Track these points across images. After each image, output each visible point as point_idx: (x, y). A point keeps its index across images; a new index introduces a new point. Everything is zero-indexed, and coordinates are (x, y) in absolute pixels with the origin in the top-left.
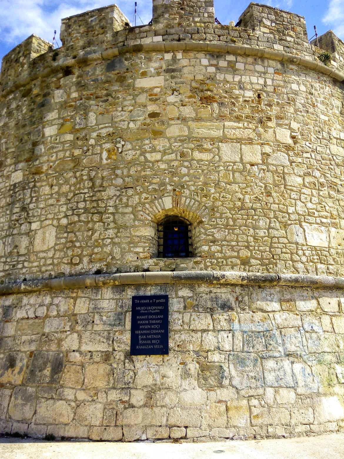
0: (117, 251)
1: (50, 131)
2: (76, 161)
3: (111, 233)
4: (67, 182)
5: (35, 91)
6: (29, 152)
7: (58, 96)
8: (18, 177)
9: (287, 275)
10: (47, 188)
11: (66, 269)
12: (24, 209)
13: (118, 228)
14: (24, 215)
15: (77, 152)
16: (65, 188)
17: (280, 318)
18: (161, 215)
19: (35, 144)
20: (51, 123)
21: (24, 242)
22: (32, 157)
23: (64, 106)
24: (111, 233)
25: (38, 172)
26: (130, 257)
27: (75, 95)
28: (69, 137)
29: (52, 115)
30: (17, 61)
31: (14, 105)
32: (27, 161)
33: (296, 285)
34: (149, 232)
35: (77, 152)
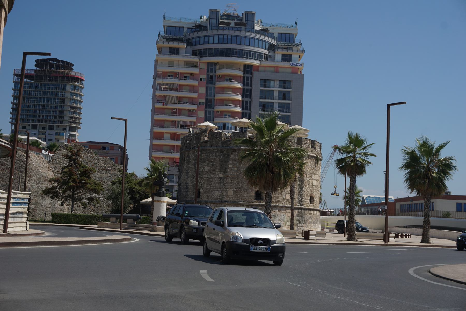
0: (247, 198)
1: (230, 166)
2: (237, 175)
3: (246, 194)
4: (235, 180)
5: (225, 153)
6: (224, 169)
7: (232, 157)
8: (221, 176)
9: (281, 205)
10: (230, 181)
11: (236, 201)
12: (224, 185)
13: (248, 193)
14: (224, 186)
15: (238, 173)
16: (235, 182)
17: (278, 213)
18: (256, 190)
19: (226, 168)
20: (231, 164)
21: (225, 193)
22: (225, 172)
23: (234, 160)
24: (246, 194)
25: (227, 176)
26: (250, 199)
27: (237, 158)
28: (236, 169)
29: (231, 162)
30: (216, 138)
31: (218, 154)
32: (224, 172)
33: (282, 207)
34: (254, 194)
35: (238, 173)
